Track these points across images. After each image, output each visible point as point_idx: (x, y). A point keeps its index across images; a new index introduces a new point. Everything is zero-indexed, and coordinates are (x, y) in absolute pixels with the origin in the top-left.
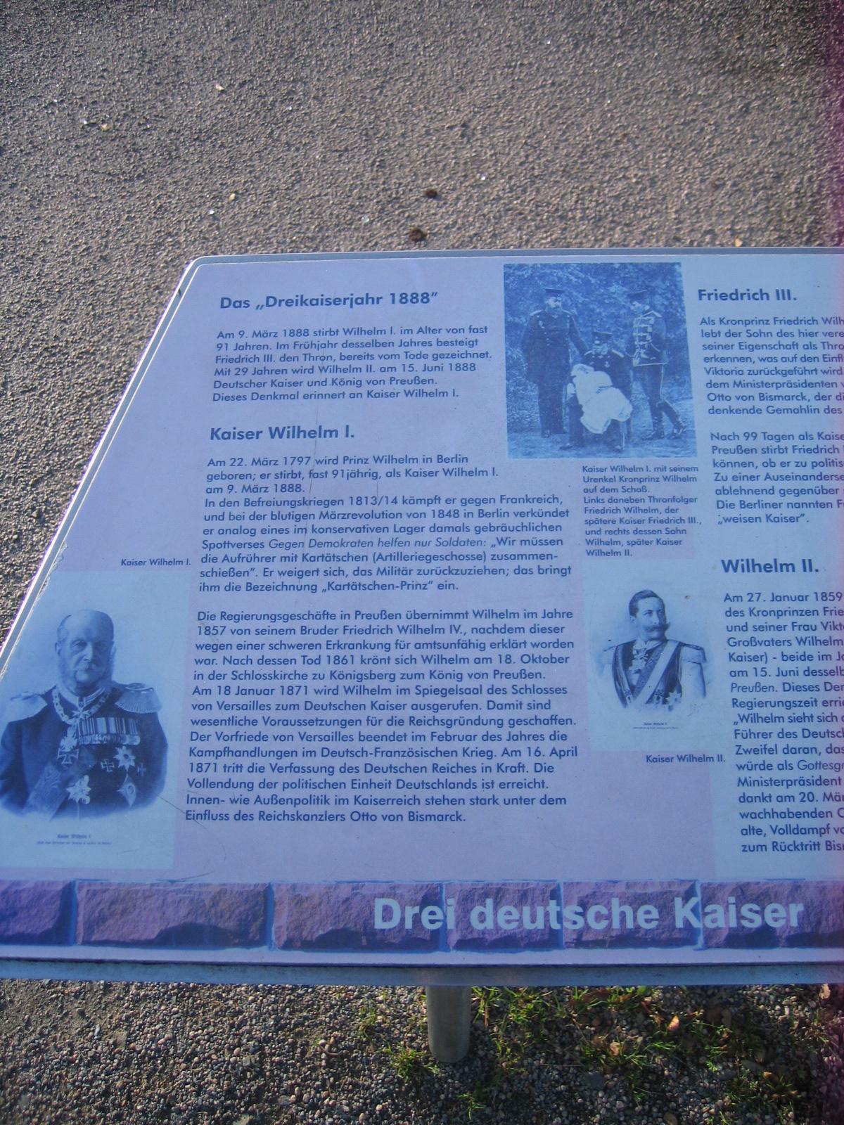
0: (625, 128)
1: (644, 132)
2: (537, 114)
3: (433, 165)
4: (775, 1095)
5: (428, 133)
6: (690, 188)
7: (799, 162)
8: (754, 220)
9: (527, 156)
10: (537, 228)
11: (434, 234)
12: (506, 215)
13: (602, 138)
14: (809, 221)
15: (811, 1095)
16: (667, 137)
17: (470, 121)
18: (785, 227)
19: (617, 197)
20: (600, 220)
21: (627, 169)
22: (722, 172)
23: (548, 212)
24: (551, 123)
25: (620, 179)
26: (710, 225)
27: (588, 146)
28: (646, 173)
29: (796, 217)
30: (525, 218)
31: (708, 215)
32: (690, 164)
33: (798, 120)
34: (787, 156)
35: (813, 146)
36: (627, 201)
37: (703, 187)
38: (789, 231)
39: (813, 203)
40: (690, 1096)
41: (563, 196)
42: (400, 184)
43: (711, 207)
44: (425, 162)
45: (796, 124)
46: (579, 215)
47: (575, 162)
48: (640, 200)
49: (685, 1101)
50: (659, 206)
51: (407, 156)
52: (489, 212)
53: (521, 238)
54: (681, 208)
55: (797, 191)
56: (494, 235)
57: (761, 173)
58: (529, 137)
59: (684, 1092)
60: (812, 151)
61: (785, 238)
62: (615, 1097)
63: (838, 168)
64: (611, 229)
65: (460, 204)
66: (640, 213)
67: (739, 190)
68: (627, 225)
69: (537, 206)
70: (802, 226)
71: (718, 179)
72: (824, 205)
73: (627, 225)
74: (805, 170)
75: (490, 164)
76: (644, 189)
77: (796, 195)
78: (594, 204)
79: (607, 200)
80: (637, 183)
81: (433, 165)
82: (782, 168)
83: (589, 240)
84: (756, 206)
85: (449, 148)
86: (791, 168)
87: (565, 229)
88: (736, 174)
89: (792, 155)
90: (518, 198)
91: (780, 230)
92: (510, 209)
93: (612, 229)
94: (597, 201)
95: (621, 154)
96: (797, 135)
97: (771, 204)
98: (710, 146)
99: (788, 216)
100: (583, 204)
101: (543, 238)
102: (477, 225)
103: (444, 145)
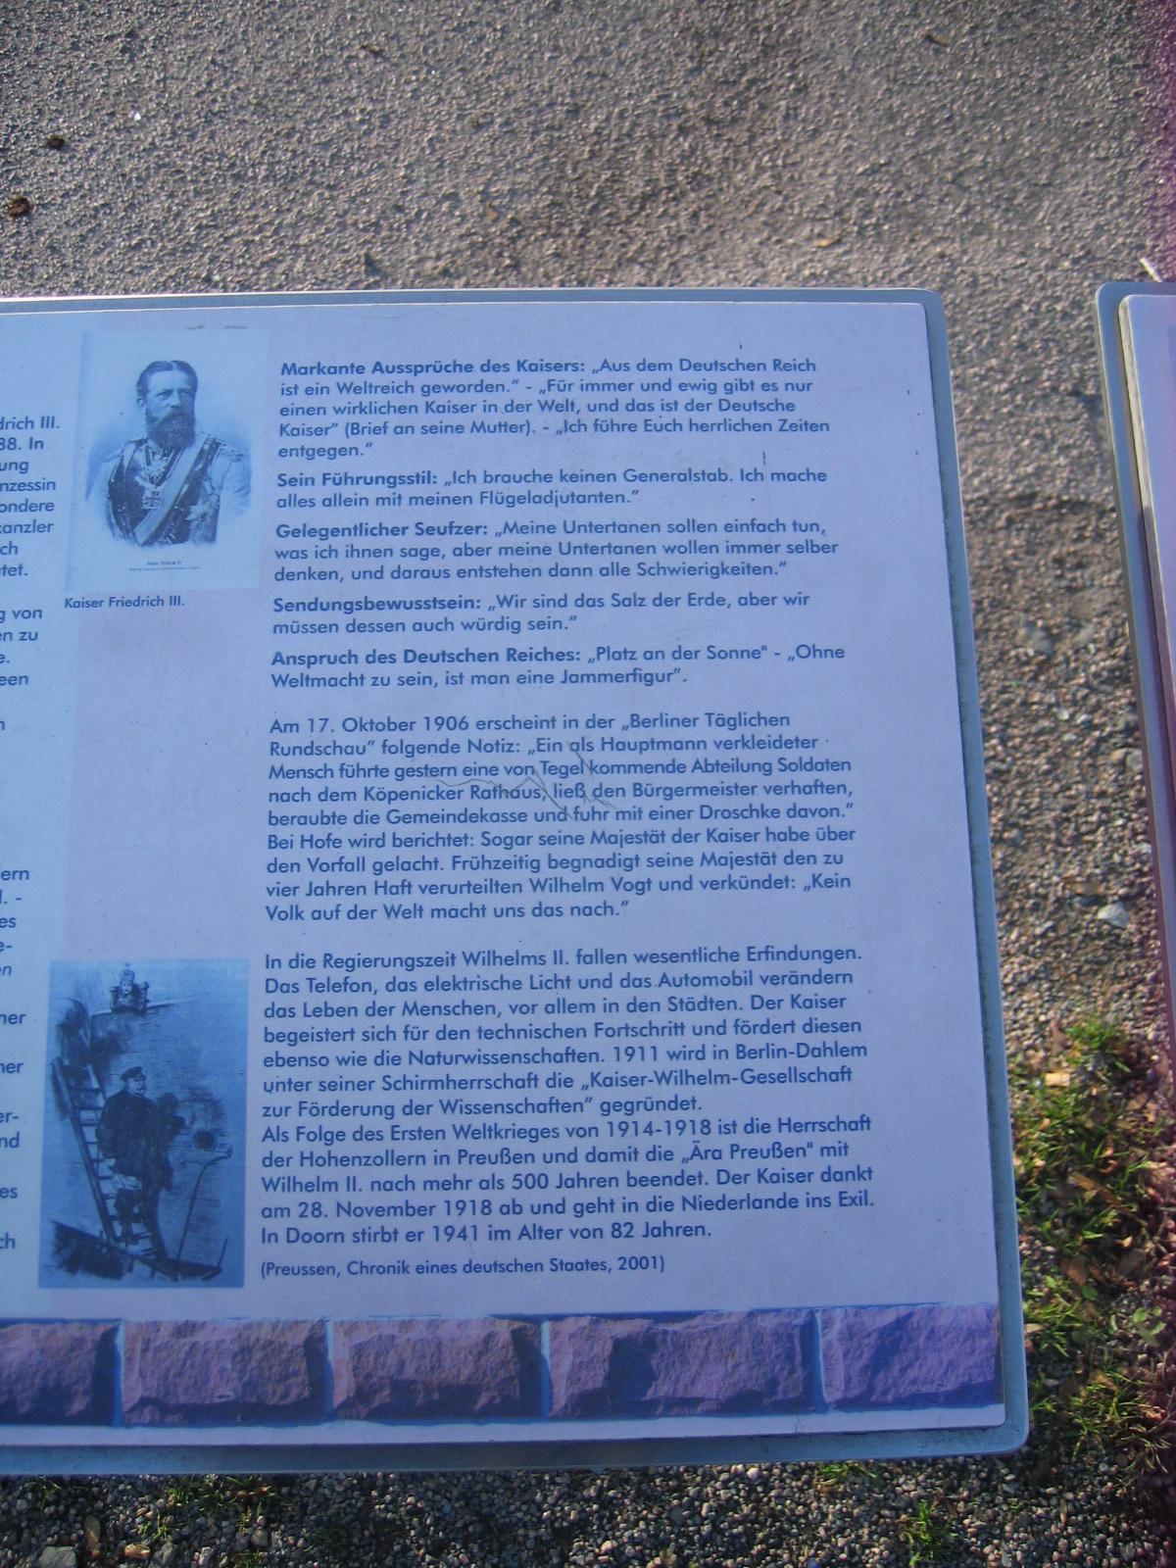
0: (367, 35)
1: (394, 43)
2: (244, 14)
3: (70, 98)
4: (241, 1493)
5: (75, 47)
7: (613, 88)
8: (523, 178)
9: (209, 84)
10: (197, 193)
11: (44, 206)
12: (157, 173)
13: (328, 52)
14: (603, 177)
15: (294, 1491)
16: (425, 50)
17: (141, 27)
18: (565, 188)
19: (326, 145)
20: (293, 180)
21: (352, 100)
22: (493, 103)
23: (219, 168)
24: (259, 29)
25: (338, 117)
26: (454, 187)
27: (304, 65)
28: (380, 106)
29: (585, 173)
30: (183, 179)
31: (455, 171)
32: (449, 91)
33: (628, 22)
34: (596, 80)
35: (640, 63)
36: (340, 150)
37: (458, 128)
38: (570, 195)
39: (616, 150)
40: (124, 1492)
41: (247, 143)
42: (14, 127)
44: (59, 93)
45: (624, 29)
46: (263, 173)
47: (279, 91)
48: (360, 148)
49: (116, 1498)
50: (385, 157)
51: (36, 83)
52: (132, 170)
53: (169, 209)
54: (418, 160)
55: (597, 132)
56: (132, 206)
57: (551, 105)
58: (221, 52)
59: (116, 1487)
60: (636, 69)
61: (561, 205)
62: (17, 1494)
63: (670, 95)
64: (305, 194)
65: (93, 159)
66: (354, 169)
67: (512, 132)
68: (330, 188)
69: (206, 159)
70: (591, 186)
71: (484, 115)
72: (634, 153)
73: (330, 188)
74: (617, 99)
75: (153, 94)
76: (368, 133)
77: (595, 138)
78: (289, 155)
79: (310, 149)
80: (362, 122)
81: (70, 98)
82: (585, 98)
83: (269, 212)
84: (530, 155)
85: (100, 71)
86: (598, 97)
87: (237, 195)
88: (514, 105)
89: (605, 76)
90: (179, 148)
91: (554, 194)
92: (164, 165)
93: (307, 194)
94: (294, 152)
95: (351, 77)
96: (620, 45)
97: (554, 152)
98: (486, 64)
99: (575, 170)
100: (273, 156)
101: (201, 210)
102: (111, 190)
103: (94, 65)
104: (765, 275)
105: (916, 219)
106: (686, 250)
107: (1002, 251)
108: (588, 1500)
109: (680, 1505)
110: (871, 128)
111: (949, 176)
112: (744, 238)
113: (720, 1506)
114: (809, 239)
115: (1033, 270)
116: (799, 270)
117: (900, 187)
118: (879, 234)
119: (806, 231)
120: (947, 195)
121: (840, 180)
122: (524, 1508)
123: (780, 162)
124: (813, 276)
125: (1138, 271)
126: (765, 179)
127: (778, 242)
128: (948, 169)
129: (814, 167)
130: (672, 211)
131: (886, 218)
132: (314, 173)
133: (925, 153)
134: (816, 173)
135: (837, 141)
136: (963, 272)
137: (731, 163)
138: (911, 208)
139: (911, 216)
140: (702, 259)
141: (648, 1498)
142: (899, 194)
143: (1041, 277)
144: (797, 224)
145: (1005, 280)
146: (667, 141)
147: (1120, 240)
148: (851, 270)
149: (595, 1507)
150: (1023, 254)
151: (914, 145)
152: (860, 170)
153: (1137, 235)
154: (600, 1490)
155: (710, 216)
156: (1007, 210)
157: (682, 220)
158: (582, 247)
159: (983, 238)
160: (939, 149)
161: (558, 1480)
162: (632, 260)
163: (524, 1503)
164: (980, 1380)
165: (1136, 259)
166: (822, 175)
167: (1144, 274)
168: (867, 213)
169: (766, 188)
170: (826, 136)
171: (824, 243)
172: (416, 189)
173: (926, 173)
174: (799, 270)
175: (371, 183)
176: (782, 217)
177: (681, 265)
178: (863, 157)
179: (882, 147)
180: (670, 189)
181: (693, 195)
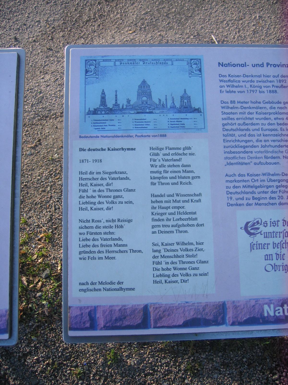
6: (38, 4)
8: (57, 16)
19: (8, 8)
31: (40, 15)
38: (68, 21)
39: (82, 9)
43: (43, 11)
48: (17, 9)
50: (23, 11)
61: (66, 23)
67: (56, 4)
68: (9, 19)
73: (9, 19)
84: (60, 10)
99: (70, 14)
104: (114, 41)
105: (155, 26)
106: (95, 34)
107: (176, 34)
108: (32, 347)
109: (54, 348)
110: (147, 2)
111: (165, 14)
112: (110, 31)
113: (64, 349)
114: (127, 31)
115: (183, 38)
116: (123, 39)
117: (153, 17)
118: (145, 30)
119: (127, 29)
120: (164, 19)
121: (137, 16)
122: (16, 348)
123: (123, 11)
124: (127, 41)
125: (211, 38)
126: (119, 16)
127: (119, 32)
128: (166, 13)
129: (131, 12)
130: (93, 24)
131: (148, 25)
132: (5, 16)
133: (160, 8)
134: (131, 14)
135: (138, 6)
136: (165, 39)
137: (110, 12)
138: (154, 23)
139: (154, 25)
140: (99, 37)
141: (47, 346)
142: (152, 19)
143: (185, 40)
144: (125, 27)
145: (175, 41)
146: (95, 6)
147: (207, 31)
148: (136, 39)
149: (34, 348)
150: (181, 34)
151: (158, 6)
152: (143, 13)
153: (212, 29)
154: (35, 345)
155: (103, 26)
156: (179, 23)
157: (95, 27)
158: (70, 34)
159: (172, 30)
160: (164, 7)
161: (25, 342)
162: (82, 37)
163: (17, 347)
164: (3, 328)
165: (211, 35)
166: (133, 15)
167: (212, 39)
168: (143, 24)
169: (118, 18)
170: (136, 4)
171: (131, 32)
172: (30, 20)
173: (160, 14)
174: (123, 39)
175: (19, 18)
176: (121, 25)
177: (94, 38)
178: (144, 10)
179: (149, 7)
180: (94, 19)
181: (99, 20)
